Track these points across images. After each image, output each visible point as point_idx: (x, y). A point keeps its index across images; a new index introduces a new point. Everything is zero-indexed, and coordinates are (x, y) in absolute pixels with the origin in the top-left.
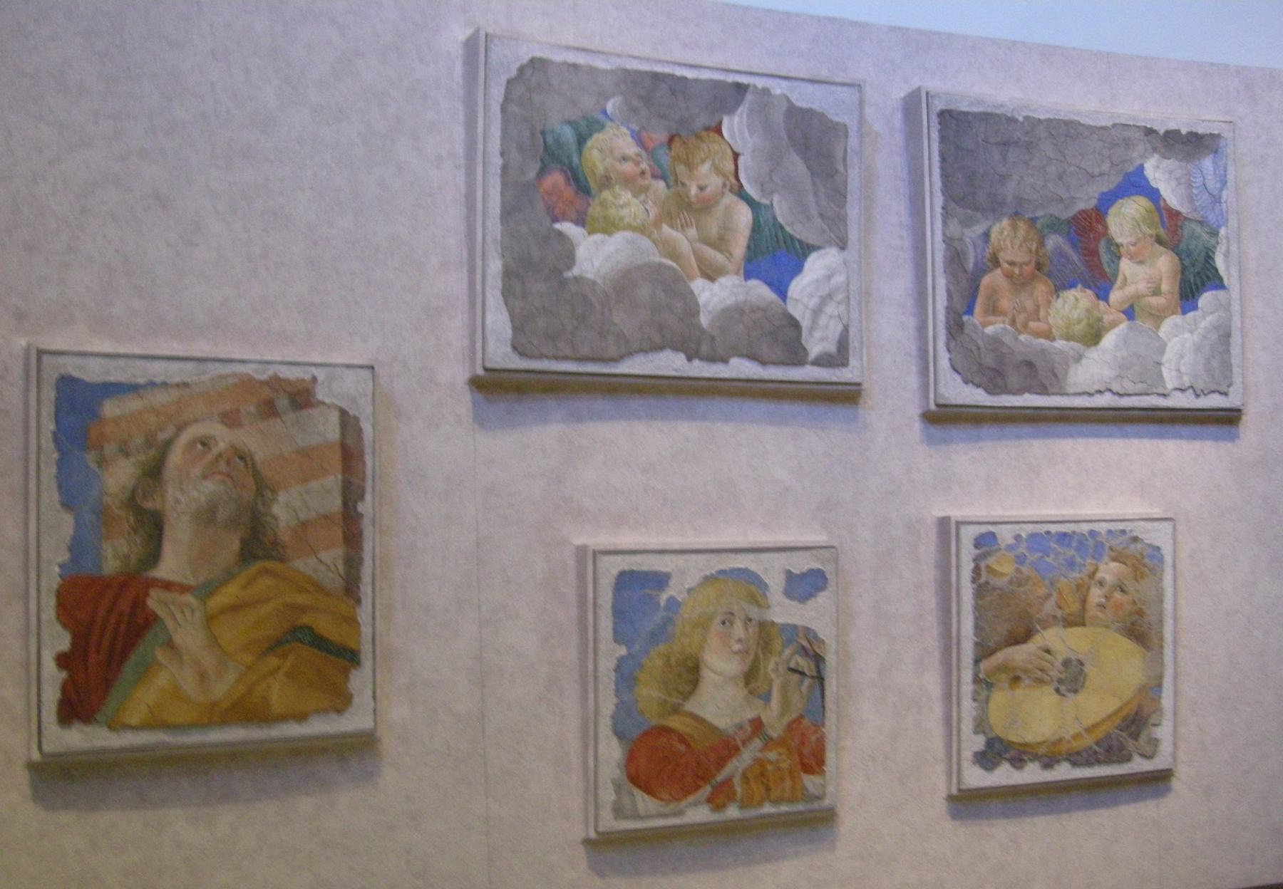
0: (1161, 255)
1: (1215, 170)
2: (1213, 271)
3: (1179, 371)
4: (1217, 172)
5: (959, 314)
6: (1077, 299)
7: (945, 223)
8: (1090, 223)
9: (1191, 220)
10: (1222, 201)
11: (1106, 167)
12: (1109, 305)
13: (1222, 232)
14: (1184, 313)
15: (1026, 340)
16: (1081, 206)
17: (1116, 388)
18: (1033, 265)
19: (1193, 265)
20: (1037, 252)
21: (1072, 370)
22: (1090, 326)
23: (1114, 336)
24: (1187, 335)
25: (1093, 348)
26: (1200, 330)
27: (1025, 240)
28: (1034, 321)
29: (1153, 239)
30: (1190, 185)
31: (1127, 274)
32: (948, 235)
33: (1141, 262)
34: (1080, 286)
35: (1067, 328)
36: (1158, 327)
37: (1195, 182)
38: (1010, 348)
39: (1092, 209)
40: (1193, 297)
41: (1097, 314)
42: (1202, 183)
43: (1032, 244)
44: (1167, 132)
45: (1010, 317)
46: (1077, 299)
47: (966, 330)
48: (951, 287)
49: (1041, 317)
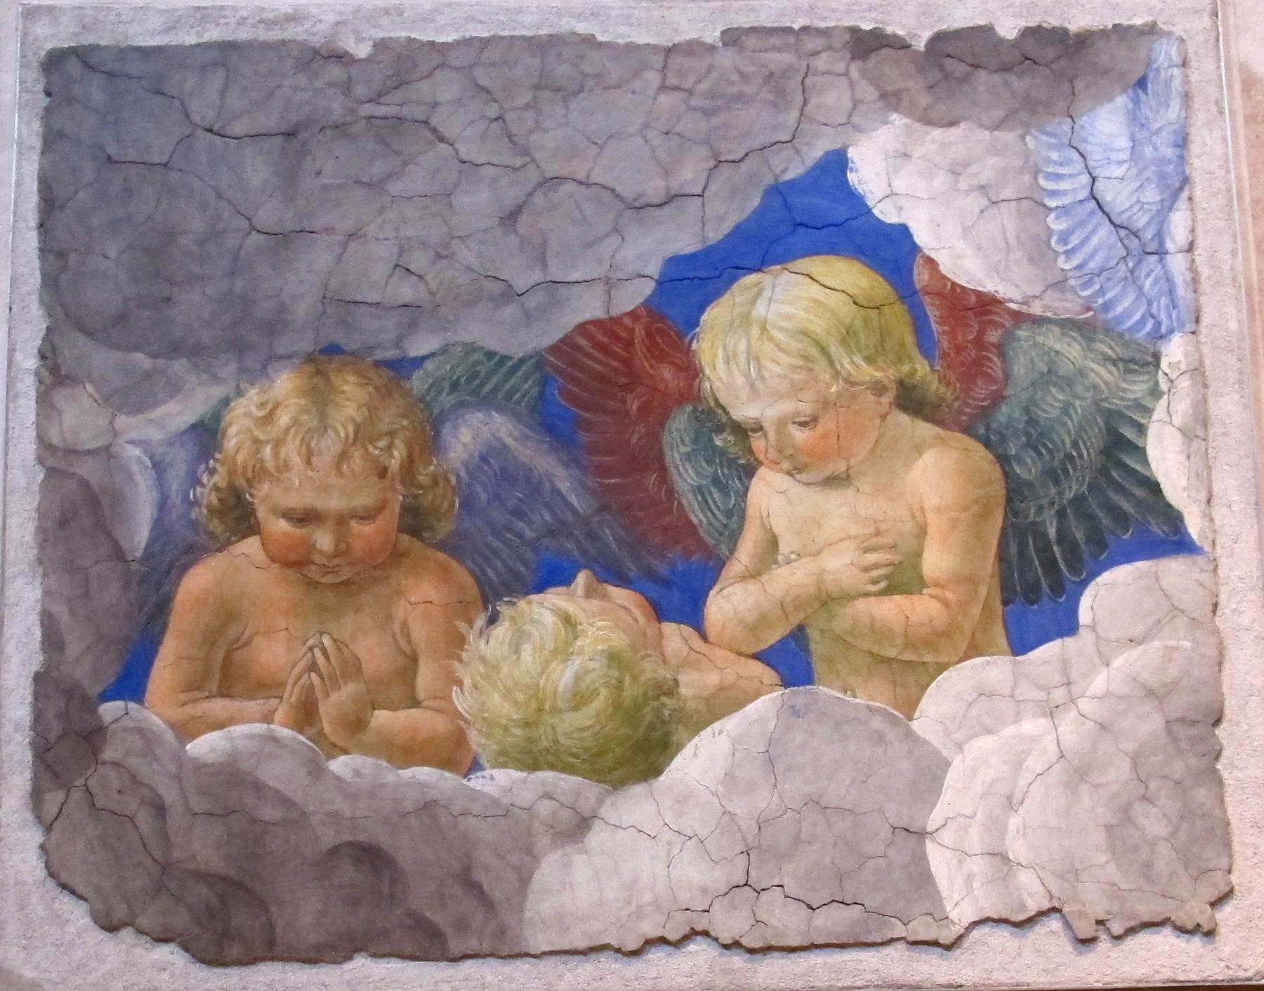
0: (919, 449)
1: (1135, 143)
2: (1140, 493)
3: (1000, 856)
4: (1148, 151)
5: (85, 699)
6: (568, 621)
7: (44, 400)
8: (628, 362)
10: (1169, 245)
11: (690, 174)
12: (704, 637)
13: (1175, 351)
14: (1020, 646)
15: (357, 773)
17: (729, 924)
19: (1054, 476)
20: (409, 467)
21: (548, 870)
22: (625, 712)
23: (724, 744)
24: (1032, 726)
25: (638, 789)
26: (1083, 704)
27: (361, 435)
28: (393, 707)
29: (888, 398)
30: (1035, 203)
31: (779, 527)
32: (55, 438)
33: (835, 481)
34: (582, 578)
35: (527, 724)
36: (910, 707)
37: (1054, 194)
38: (286, 802)
39: (633, 315)
40: (1058, 587)
41: (652, 670)
42: (1084, 194)
43: (390, 447)
44: (940, 38)
45: (292, 694)
46: (568, 621)
47: (109, 753)
48: (60, 609)
49: (421, 694)
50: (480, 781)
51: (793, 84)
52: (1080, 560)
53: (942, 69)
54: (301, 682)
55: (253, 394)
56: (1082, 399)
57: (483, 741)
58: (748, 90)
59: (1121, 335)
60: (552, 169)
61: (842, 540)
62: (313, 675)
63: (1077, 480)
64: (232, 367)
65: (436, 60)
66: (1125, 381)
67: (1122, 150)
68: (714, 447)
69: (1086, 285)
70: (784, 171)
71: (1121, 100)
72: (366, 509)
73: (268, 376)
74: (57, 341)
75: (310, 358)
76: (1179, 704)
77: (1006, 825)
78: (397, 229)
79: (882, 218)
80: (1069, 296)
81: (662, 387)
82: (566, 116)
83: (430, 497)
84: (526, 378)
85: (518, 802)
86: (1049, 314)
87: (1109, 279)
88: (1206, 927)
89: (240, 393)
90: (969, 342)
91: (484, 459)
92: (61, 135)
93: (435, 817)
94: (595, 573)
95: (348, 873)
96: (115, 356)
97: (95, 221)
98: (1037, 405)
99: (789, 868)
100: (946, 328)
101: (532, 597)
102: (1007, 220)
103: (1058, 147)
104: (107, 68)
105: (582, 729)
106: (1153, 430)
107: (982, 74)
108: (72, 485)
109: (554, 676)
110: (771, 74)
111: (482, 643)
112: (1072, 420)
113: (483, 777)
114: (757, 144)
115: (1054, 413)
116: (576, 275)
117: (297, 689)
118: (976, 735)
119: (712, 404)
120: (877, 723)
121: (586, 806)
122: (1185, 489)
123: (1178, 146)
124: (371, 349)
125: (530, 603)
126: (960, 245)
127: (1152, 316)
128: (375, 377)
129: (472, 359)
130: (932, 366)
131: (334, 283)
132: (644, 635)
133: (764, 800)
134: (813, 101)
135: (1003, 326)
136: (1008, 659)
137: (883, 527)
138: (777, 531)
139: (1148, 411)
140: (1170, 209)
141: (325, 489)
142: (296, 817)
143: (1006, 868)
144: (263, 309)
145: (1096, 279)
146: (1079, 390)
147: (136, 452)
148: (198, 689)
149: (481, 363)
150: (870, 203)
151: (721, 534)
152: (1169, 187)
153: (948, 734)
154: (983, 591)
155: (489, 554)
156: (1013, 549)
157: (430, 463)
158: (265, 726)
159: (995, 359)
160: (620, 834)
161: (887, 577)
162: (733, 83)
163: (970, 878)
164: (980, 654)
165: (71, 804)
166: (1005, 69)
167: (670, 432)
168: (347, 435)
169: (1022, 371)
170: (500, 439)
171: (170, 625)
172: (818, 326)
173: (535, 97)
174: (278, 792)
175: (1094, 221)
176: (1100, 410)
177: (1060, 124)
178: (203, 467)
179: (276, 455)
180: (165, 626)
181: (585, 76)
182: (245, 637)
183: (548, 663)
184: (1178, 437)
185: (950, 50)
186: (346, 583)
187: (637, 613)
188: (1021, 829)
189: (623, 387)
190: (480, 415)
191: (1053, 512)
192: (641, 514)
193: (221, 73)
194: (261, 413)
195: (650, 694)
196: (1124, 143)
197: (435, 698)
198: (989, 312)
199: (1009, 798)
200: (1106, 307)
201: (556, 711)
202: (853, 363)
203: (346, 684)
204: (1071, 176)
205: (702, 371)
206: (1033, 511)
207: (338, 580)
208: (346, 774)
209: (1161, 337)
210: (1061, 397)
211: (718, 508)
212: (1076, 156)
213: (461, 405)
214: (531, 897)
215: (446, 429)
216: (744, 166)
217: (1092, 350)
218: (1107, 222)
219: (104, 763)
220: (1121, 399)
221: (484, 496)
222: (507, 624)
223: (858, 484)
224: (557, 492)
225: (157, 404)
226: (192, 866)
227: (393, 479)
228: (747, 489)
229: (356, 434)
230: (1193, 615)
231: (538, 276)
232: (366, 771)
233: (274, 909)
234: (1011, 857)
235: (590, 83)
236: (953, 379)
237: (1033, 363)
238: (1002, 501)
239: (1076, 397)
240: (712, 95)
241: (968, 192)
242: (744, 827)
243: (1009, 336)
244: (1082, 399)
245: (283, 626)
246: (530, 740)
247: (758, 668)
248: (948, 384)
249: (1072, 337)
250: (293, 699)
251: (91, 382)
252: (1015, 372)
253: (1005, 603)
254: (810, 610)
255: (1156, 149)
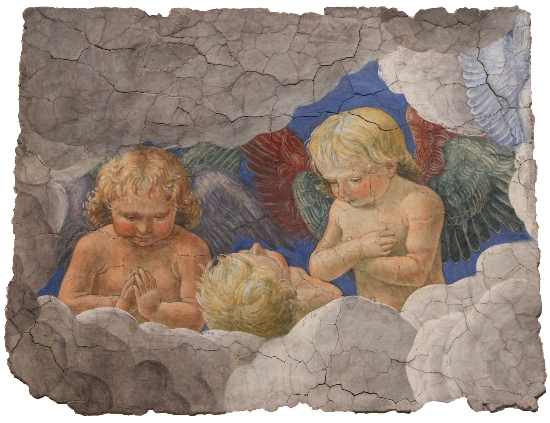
4: (512, 63)
5: (32, 294)
6: (248, 265)
8: (278, 152)
9: (460, 137)
10: (521, 105)
11: (308, 71)
12: (309, 274)
14: (449, 281)
16: (262, 128)
18: (172, 217)
19: (467, 205)
22: (273, 306)
23: (316, 321)
24: (454, 315)
25: (278, 340)
26: (478, 306)
27: (161, 181)
28: (169, 301)
31: (343, 225)
32: (23, 179)
33: (368, 206)
34: (255, 246)
35: (229, 310)
36: (400, 306)
37: (470, 81)
38: (121, 342)
39: (281, 132)
40: (467, 255)
41: (285, 287)
42: (483, 81)
43: (173, 186)
45: (125, 294)
46: (248, 265)
49: (182, 296)
50: (207, 335)
51: (355, 32)
52: (478, 242)
53: (421, 26)
54: (129, 289)
55: (112, 162)
56: (480, 171)
57: (209, 317)
58: (336, 35)
59: (498, 144)
60: (247, 67)
61: (370, 232)
62: (134, 286)
63: (477, 207)
64: (104, 150)
65: (198, 18)
66: (499, 164)
67: (501, 63)
68: (315, 190)
69: (483, 121)
70: (350, 70)
71: (501, 40)
72: (161, 214)
73: (119, 155)
74: (27, 136)
75: (138, 147)
76: (521, 308)
77: (442, 360)
78: (179, 92)
79: (393, 91)
80: (475, 126)
81: (293, 164)
82: (255, 44)
83: (189, 209)
84: (234, 158)
85: (224, 344)
86: (466, 134)
87: (493, 119)
88: (533, 408)
89: (107, 162)
90: (429, 146)
91: (213, 193)
92: (30, 46)
93: (186, 350)
94: (261, 245)
95: (147, 374)
96: (50, 144)
97: (45, 84)
98: (459, 174)
99: (344, 376)
100: (420, 140)
101: (233, 254)
102: (448, 93)
103: (472, 61)
104: (52, 17)
105: (253, 313)
106: (511, 185)
107: (439, 28)
108: (29, 199)
109: (241, 289)
110: (346, 27)
111: (210, 274)
112: (475, 181)
113: (209, 333)
114: (338, 58)
115: (467, 178)
116: (257, 114)
117: (127, 293)
118: (429, 319)
119: (315, 171)
120: (385, 313)
121: (254, 347)
122: (526, 212)
123: (526, 61)
124: (166, 144)
125: (232, 257)
126: (427, 103)
127: (513, 136)
128: (167, 156)
129: (209, 150)
130: (413, 156)
131: (150, 115)
132: (282, 272)
133: (332, 346)
134: (364, 39)
135: (445, 139)
136: (444, 285)
137: (389, 226)
138: (342, 228)
139: (510, 177)
140: (522, 88)
141: (144, 205)
142: (125, 350)
143: (442, 379)
144: (117, 126)
145: (487, 119)
146: (479, 168)
147: (59, 186)
148: (83, 291)
149: (214, 151)
150: (388, 85)
151: (317, 228)
152: (521, 79)
153: (417, 318)
154: (434, 255)
155: (214, 234)
156: (448, 237)
157: (190, 194)
158: (113, 308)
159: (441, 153)
160: (269, 360)
161: (390, 249)
162: (329, 31)
163: (425, 383)
164: (432, 284)
165: (23, 340)
166: (450, 26)
167: (296, 182)
168: (153, 182)
169: (453, 159)
170: (221, 185)
171: (71, 263)
172: (363, 138)
173: (241, 36)
174: (116, 337)
175: (487, 93)
176: (488, 176)
177: (473, 51)
178: (89, 193)
179: (122, 189)
180: (69, 263)
181: (264, 27)
182: (104, 269)
183: (239, 283)
184: (523, 189)
185: (425, 18)
186: (151, 246)
187: (279, 262)
188: (449, 361)
189: (276, 163)
190: (212, 174)
191: (466, 221)
192: (282, 219)
193: (103, 21)
194: (115, 171)
195: (284, 298)
196: (502, 59)
197: (189, 297)
198: (439, 133)
199: (444, 348)
200: (492, 131)
201: (242, 304)
202: (378, 155)
203: (149, 290)
204: (477, 74)
205: (311, 157)
206: (457, 221)
207: (147, 245)
208: (148, 331)
209: (516, 145)
210: (470, 171)
211: (316, 217)
212: (480, 65)
213: (204, 169)
214: (228, 387)
215: (197, 179)
216: (332, 68)
217: (485, 150)
218: (493, 94)
219: (39, 323)
220: (498, 172)
221: (213, 209)
222: (221, 266)
223: (379, 207)
224: (245, 208)
225: (69, 165)
226: (76, 369)
227: (173, 201)
228: (330, 208)
229: (157, 181)
230: (528, 268)
231: (240, 114)
232: (156, 329)
233: (112, 390)
234: (444, 374)
235: (266, 30)
236: (422, 162)
237: (458, 155)
238: (443, 216)
239: (477, 170)
240: (319, 36)
241: (431, 80)
242: (324, 358)
243: (447, 142)
244: (480, 171)
245: (122, 264)
246: (230, 317)
247: (332, 287)
248: (420, 165)
249: (477, 145)
250: (125, 296)
251: (40, 155)
252: (450, 159)
253: (443, 261)
254: (356, 263)
255: (516, 62)
